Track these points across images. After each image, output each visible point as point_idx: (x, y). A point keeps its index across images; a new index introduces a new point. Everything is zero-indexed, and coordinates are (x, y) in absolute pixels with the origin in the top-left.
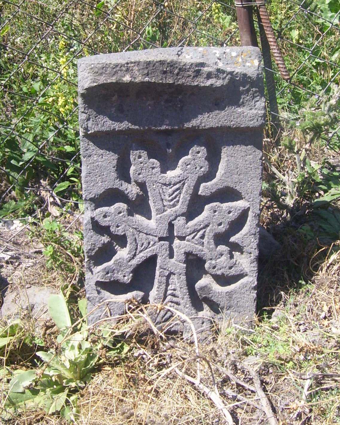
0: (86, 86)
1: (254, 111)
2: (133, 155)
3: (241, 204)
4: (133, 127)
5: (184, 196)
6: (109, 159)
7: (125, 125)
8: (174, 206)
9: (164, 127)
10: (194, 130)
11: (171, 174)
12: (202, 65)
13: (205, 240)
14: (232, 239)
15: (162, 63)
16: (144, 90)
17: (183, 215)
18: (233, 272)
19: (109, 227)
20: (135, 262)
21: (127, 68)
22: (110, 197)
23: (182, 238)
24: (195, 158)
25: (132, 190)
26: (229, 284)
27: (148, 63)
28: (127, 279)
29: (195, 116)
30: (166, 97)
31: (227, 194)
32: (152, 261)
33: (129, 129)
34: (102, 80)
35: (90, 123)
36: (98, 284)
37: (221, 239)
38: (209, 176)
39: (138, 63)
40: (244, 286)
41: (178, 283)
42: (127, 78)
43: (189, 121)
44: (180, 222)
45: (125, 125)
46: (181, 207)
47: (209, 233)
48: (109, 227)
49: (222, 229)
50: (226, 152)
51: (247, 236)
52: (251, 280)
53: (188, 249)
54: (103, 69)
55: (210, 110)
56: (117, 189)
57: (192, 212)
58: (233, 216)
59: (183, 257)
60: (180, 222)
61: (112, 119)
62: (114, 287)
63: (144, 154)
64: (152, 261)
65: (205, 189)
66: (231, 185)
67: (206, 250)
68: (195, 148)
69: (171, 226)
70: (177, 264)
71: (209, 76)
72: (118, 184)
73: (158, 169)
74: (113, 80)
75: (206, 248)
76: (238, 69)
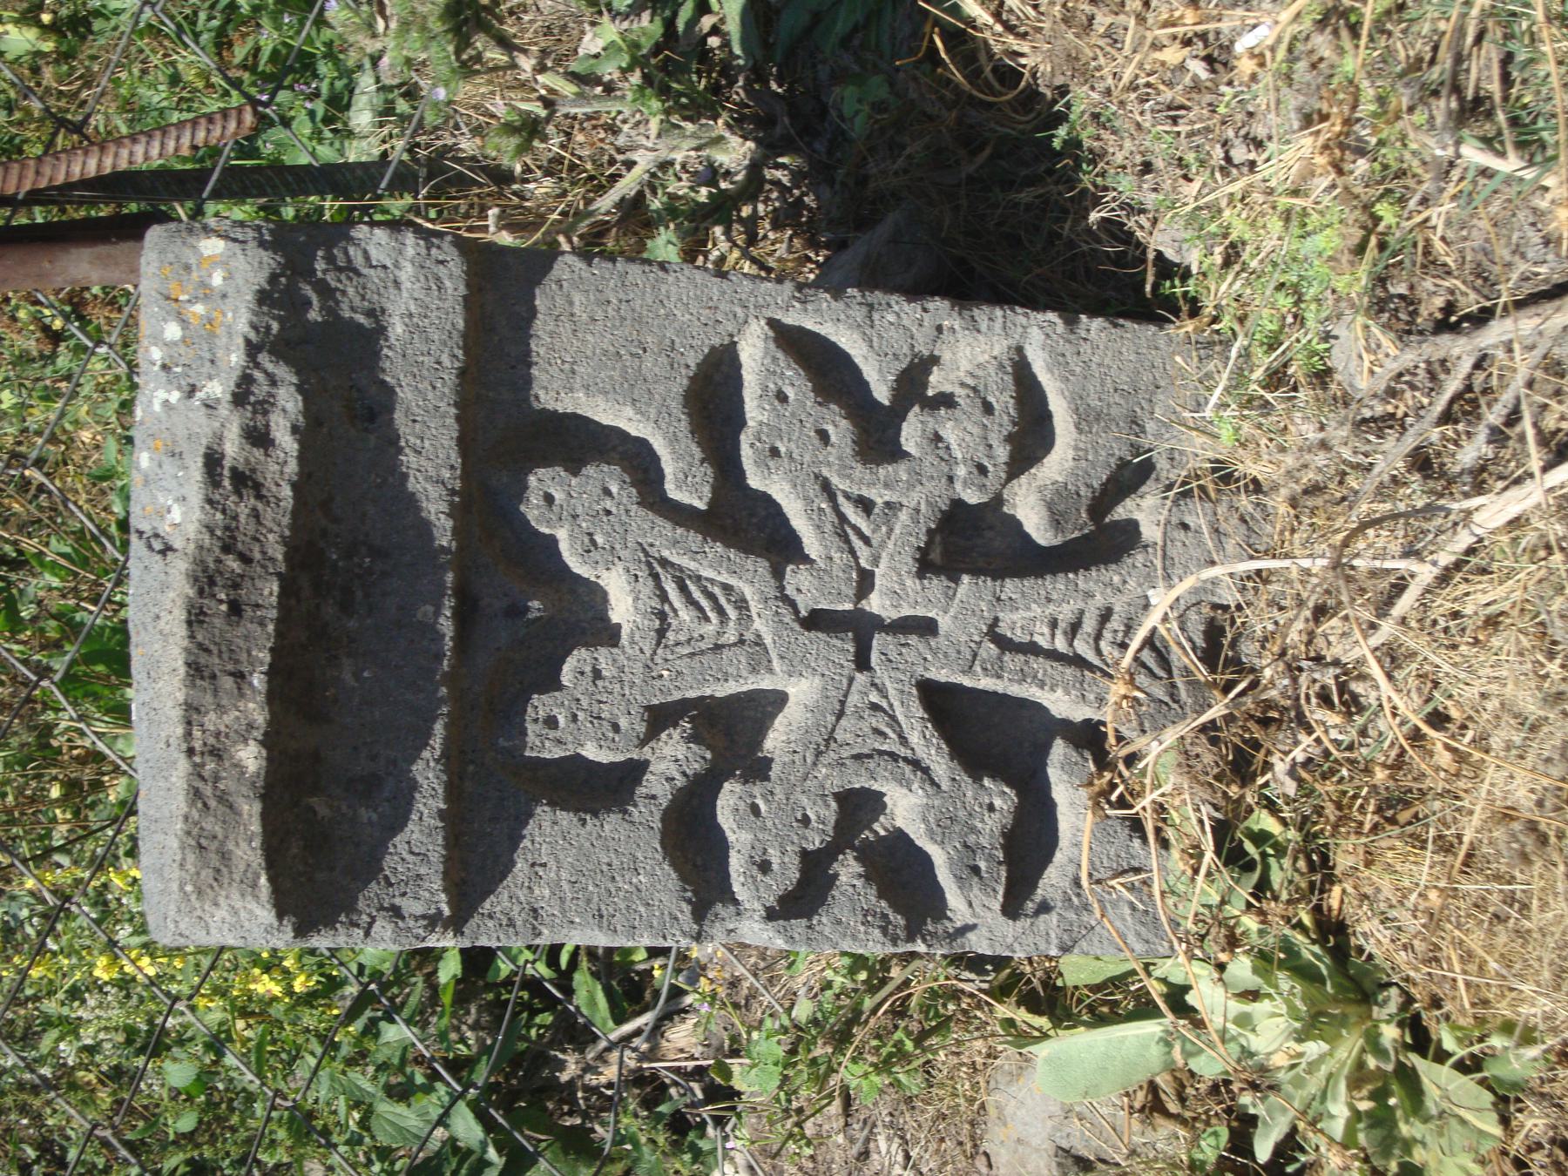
0: (266, 915)
1: (406, 273)
2: (542, 746)
3: (753, 351)
4: (437, 742)
5: (712, 563)
6: (550, 833)
7: (428, 774)
8: (742, 605)
9: (446, 626)
10: (465, 507)
11: (623, 608)
12: (213, 461)
13: (879, 496)
14: (882, 393)
15: (196, 618)
16: (295, 691)
17: (778, 574)
18: (1004, 399)
19: (804, 854)
20: (941, 765)
21: (206, 755)
22: (693, 843)
23: (865, 582)
24: (569, 511)
25: (673, 759)
26: (1047, 417)
27: (196, 670)
28: (1003, 798)
29: (411, 502)
30: (329, 611)
31: (713, 400)
32: (942, 703)
33: (446, 756)
34: (248, 853)
35: (411, 907)
36: (1012, 909)
37: (877, 438)
39: (192, 712)
40: (1058, 360)
41: (1031, 609)
42: (250, 757)
43: (425, 528)
44: (804, 587)
45: (428, 774)
46: (748, 578)
47: (851, 479)
48: (804, 854)
49: (840, 429)
50: (559, 390)
51: (872, 335)
52: (1037, 335)
53: (908, 563)
54: (204, 846)
55: (392, 443)
56: (666, 816)
57: (772, 541)
58: (797, 385)
59: (936, 585)
60: (804, 587)
61: (397, 822)
62: (1029, 844)
63: (541, 704)
64: (942, 703)
65: (687, 484)
66: (680, 384)
67: (916, 497)
68: (532, 509)
69: (817, 621)
70: (961, 607)
71: (258, 437)
73: (603, 656)
74: (251, 810)
75: (910, 496)
76: (239, 320)
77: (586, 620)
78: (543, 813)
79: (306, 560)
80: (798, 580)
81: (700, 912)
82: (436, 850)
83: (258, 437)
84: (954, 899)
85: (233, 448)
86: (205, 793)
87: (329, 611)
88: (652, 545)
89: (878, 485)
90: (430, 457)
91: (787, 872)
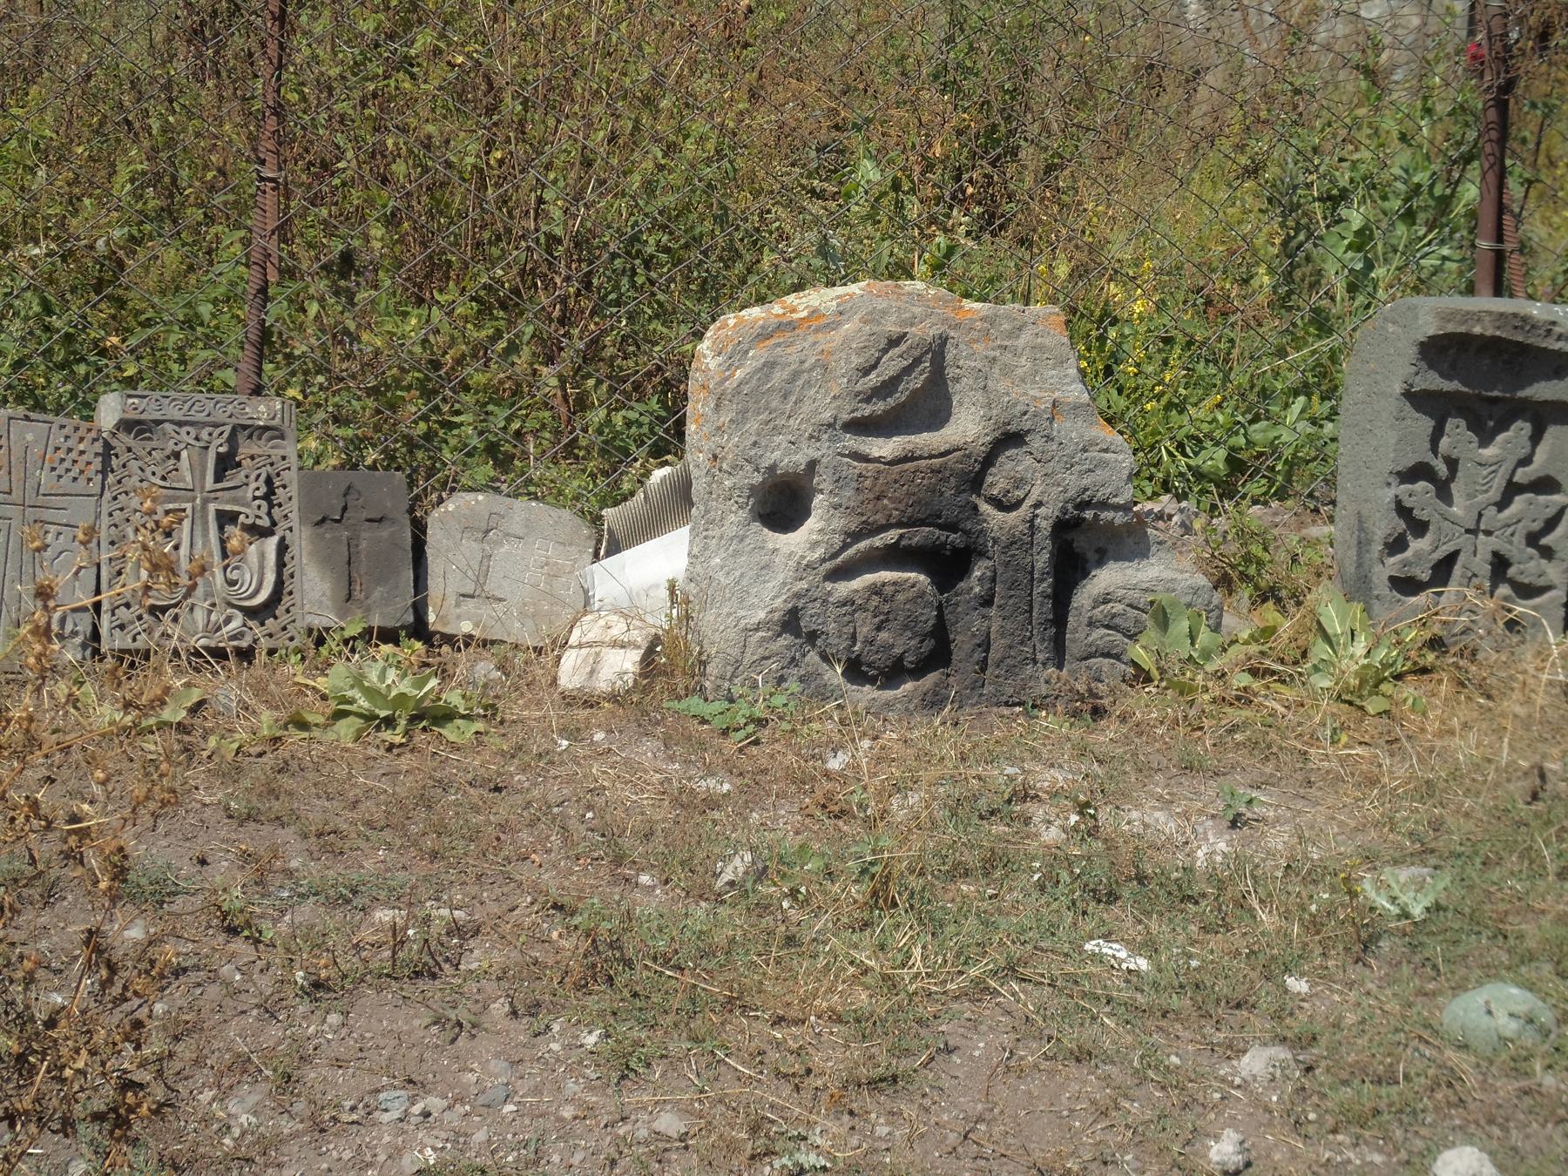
0: (1431, 332)
2: (1450, 424)
5: (1499, 483)
6: (1426, 424)
7: (1453, 386)
8: (1486, 491)
9: (1496, 393)
10: (1526, 401)
11: (1490, 452)
12: (1554, 323)
13: (1515, 539)
14: (1544, 541)
15: (1515, 315)
16: (1491, 346)
17: (1495, 504)
18: (1541, 582)
19: (1411, 509)
21: (1477, 317)
23: (1488, 533)
25: (1442, 469)
27: (1502, 314)
28: (1425, 576)
29: (1530, 384)
30: (1506, 357)
32: (1451, 559)
33: (1458, 392)
34: (1451, 328)
35: (1418, 379)
36: (1392, 579)
37: (1532, 539)
38: (1526, 461)
39: (1489, 313)
40: (1553, 600)
42: (1477, 330)
43: (1523, 388)
45: (1453, 386)
46: (1495, 494)
47: (1521, 530)
48: (1411, 509)
49: (1536, 526)
53: (1496, 548)
54: (1447, 316)
55: (1549, 379)
56: (1427, 464)
57: (1502, 504)
58: (1550, 512)
59: (1489, 557)
61: (1442, 375)
63: (1463, 423)
65: (1522, 475)
66: (1552, 473)
67: (1515, 552)
68: (1519, 424)
69: (1480, 515)
72: (1428, 457)
73: (1475, 445)
74: (1462, 329)
75: (1516, 549)
77: (1485, 441)
78: (1433, 423)
79: (1523, 349)
80: (1493, 509)
81: (1399, 473)
82: (1433, 387)
83: (1559, 338)
84: (1392, 560)
85: (1557, 330)
86: (1468, 316)
87: (1506, 357)
88: (175, 619)
89: (1519, 539)
90: (1543, 390)
91: (1408, 503)
